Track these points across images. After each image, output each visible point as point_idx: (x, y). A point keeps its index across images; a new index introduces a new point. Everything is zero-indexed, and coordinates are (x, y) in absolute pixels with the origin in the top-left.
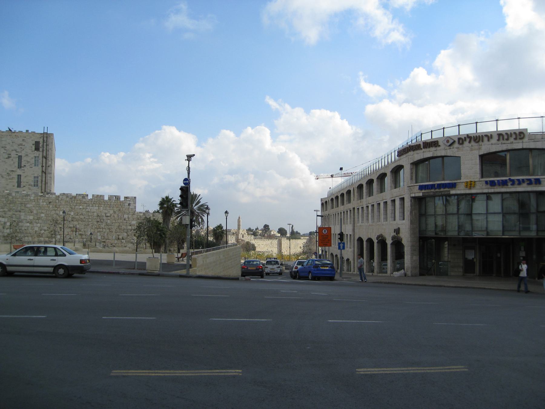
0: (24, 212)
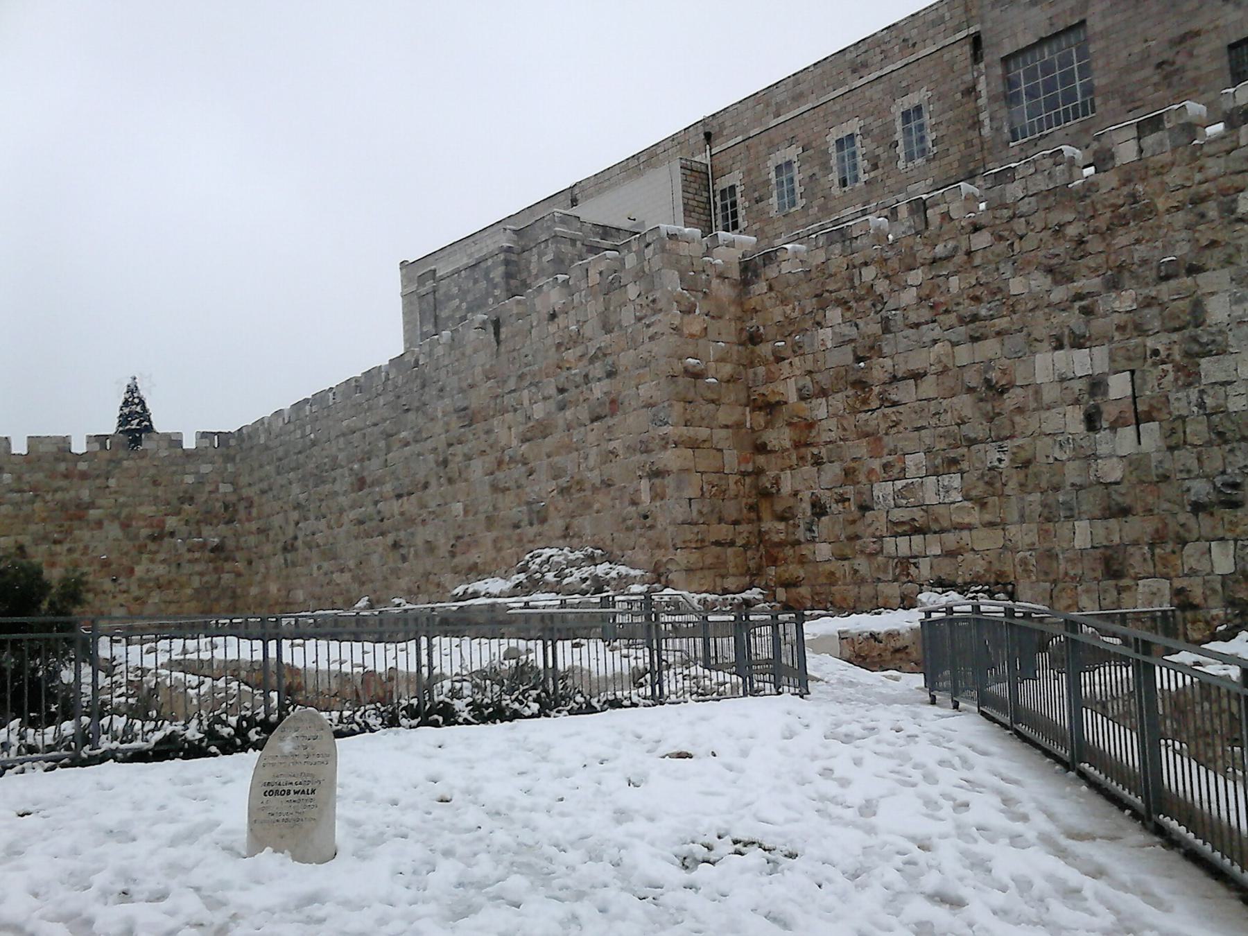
0: (1229, 261)
